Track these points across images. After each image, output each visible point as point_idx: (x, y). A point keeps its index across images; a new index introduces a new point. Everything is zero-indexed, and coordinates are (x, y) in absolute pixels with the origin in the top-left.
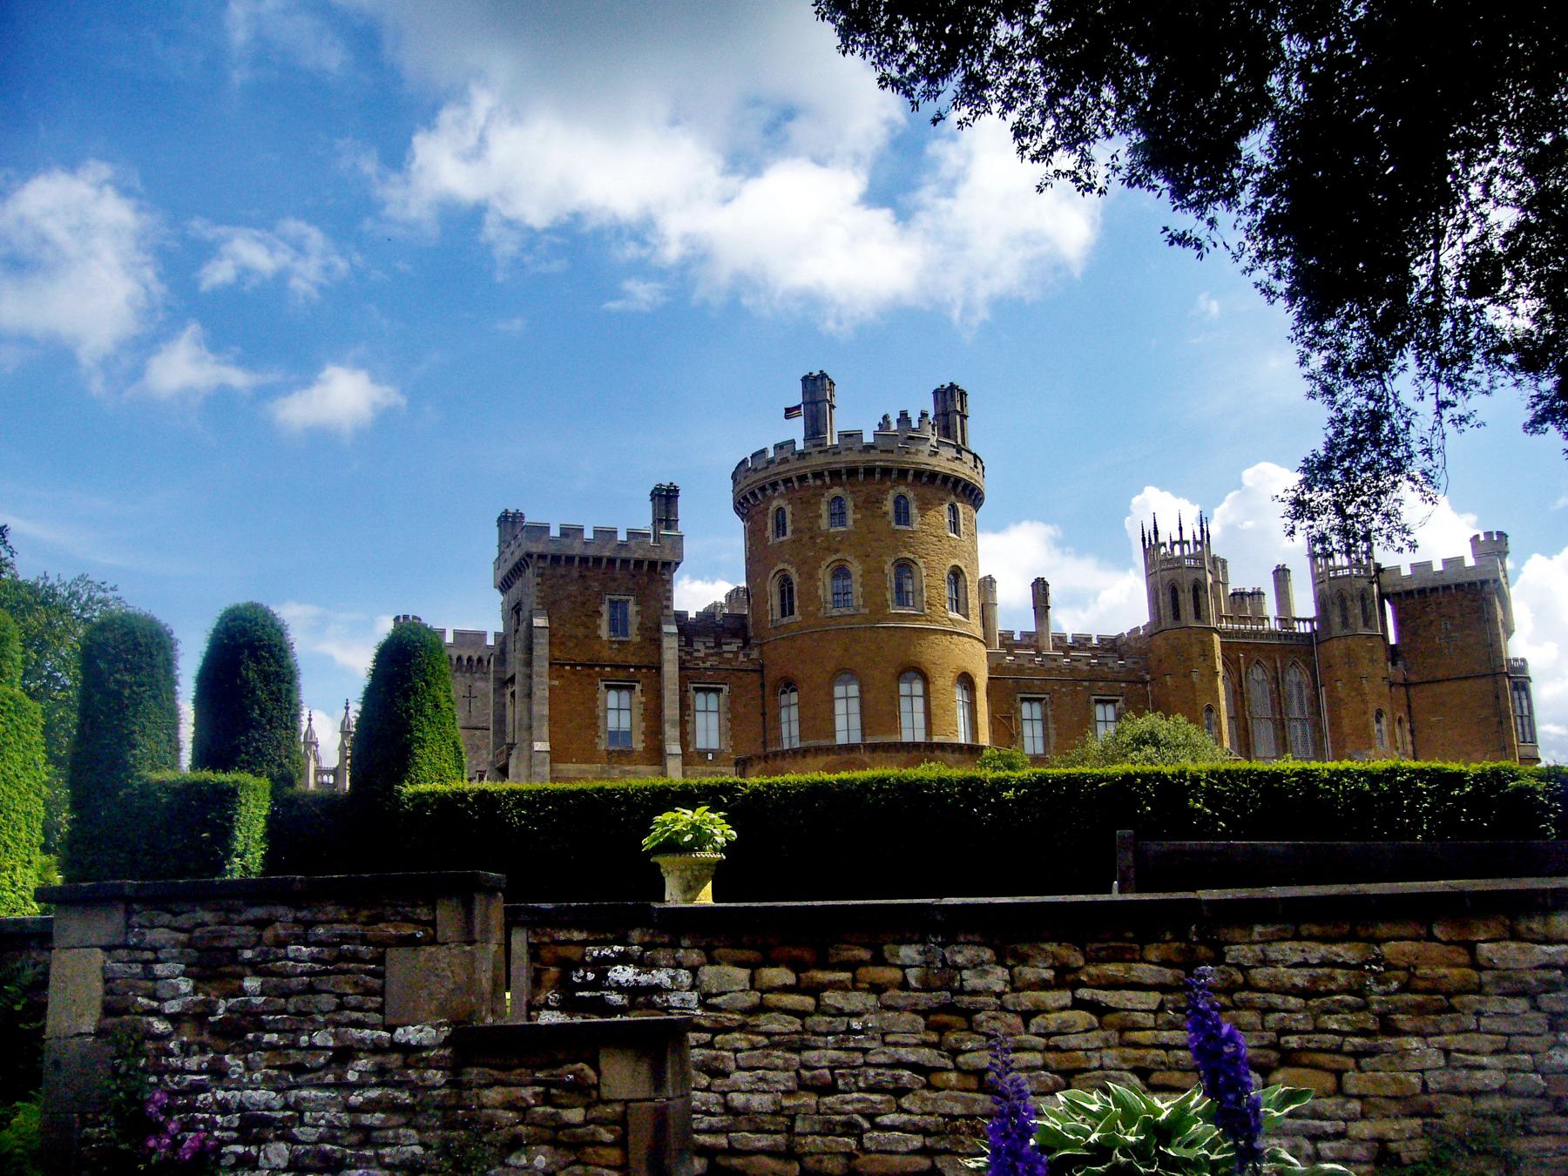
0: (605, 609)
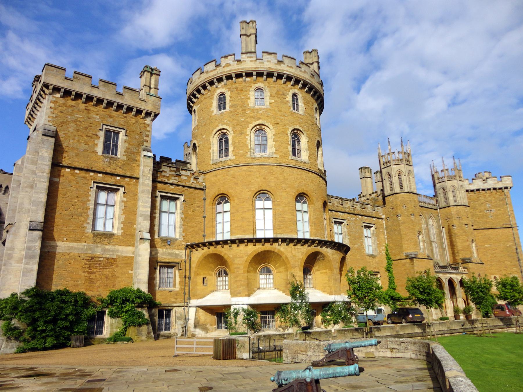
0: (102, 134)
